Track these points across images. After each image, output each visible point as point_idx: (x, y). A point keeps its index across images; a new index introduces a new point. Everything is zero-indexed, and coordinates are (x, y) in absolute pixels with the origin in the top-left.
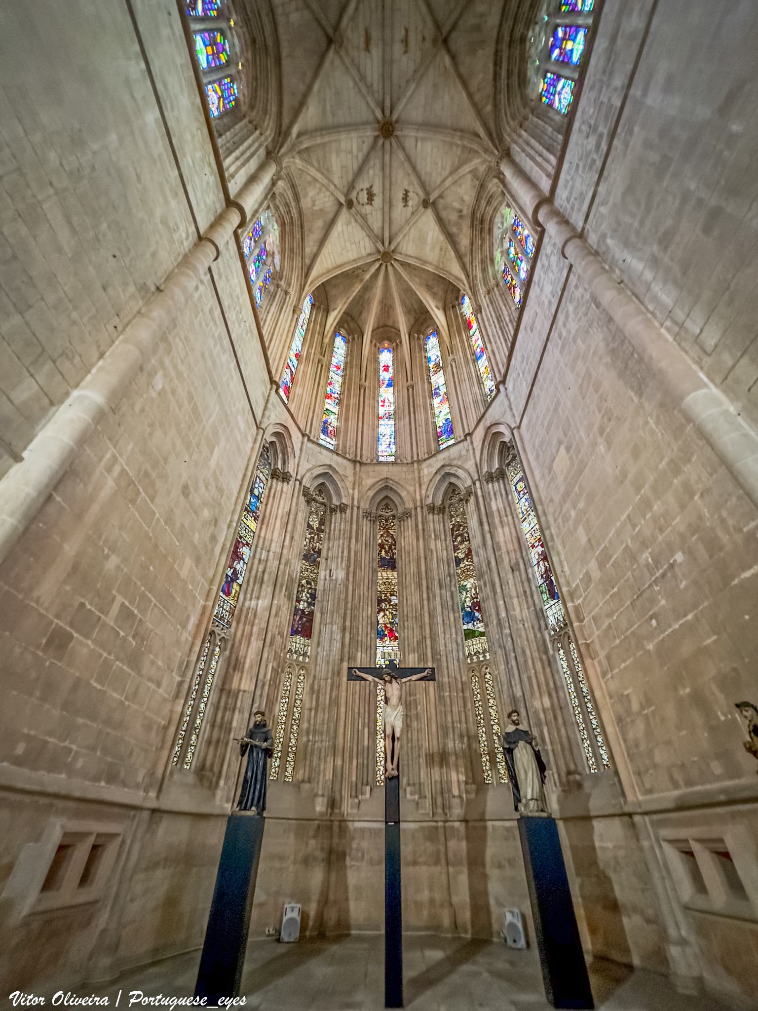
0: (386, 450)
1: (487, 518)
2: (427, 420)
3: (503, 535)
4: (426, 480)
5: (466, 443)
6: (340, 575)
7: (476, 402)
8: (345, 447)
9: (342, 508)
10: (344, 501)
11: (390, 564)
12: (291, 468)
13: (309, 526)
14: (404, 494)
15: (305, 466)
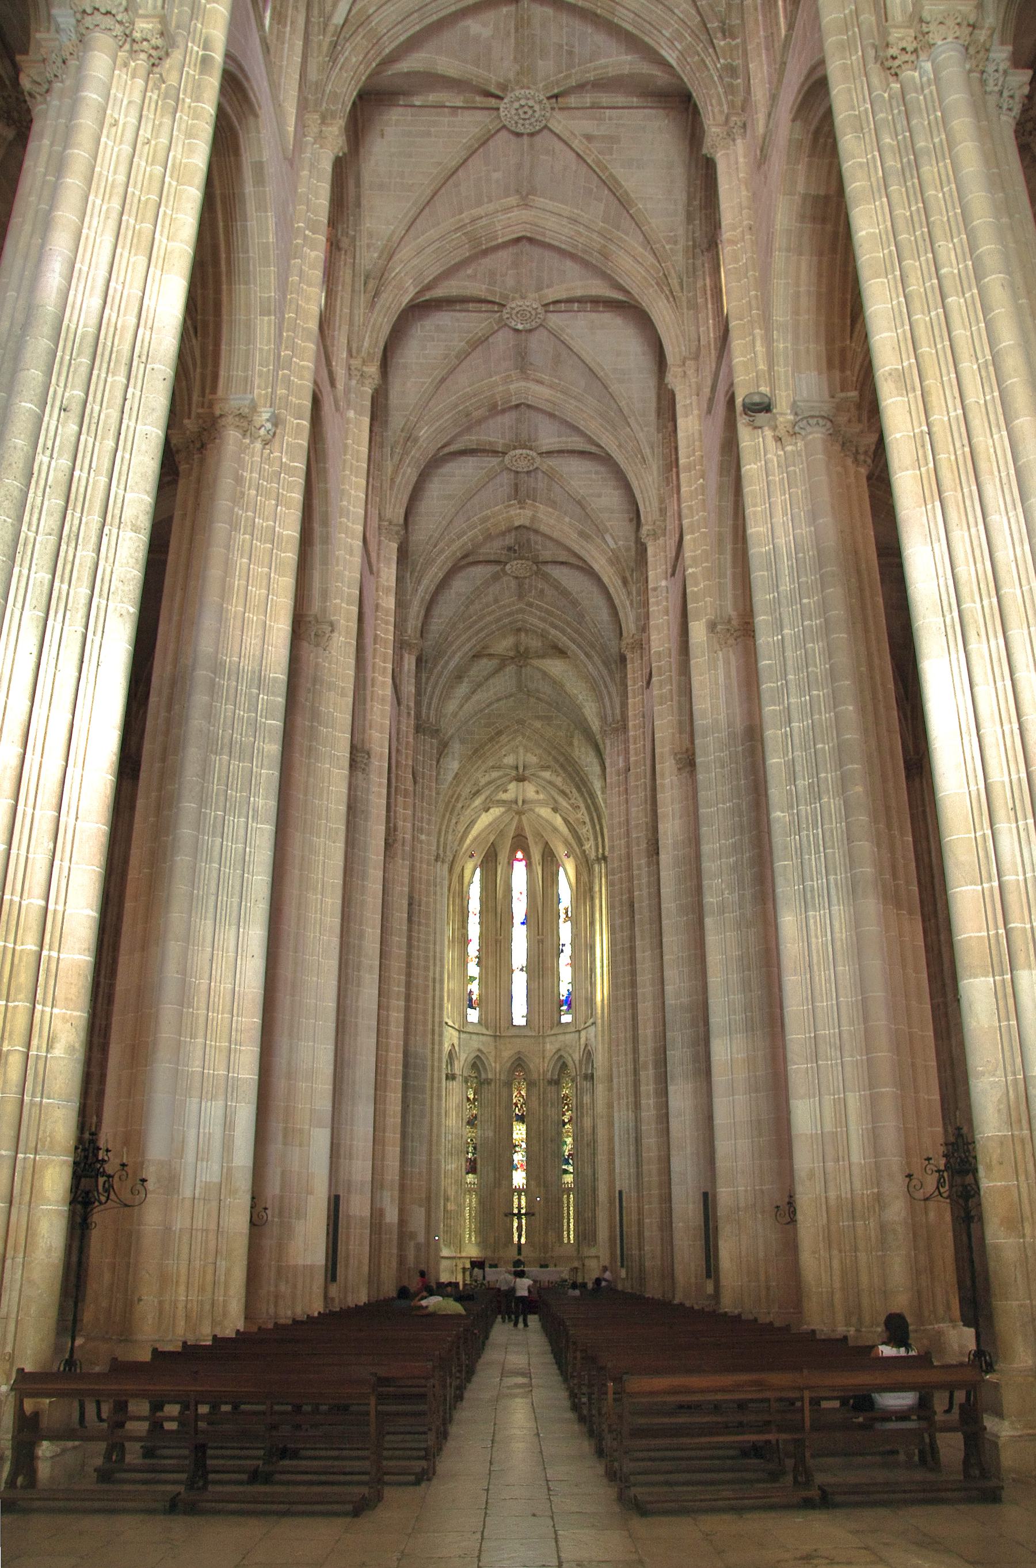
0: (519, 1014)
1: (580, 1107)
2: (553, 987)
3: (587, 1122)
4: (548, 1055)
5: (577, 1034)
6: (491, 1134)
7: (586, 999)
8: (486, 1020)
9: (488, 1082)
10: (490, 1076)
11: (521, 1119)
12: (457, 1071)
13: (468, 1099)
14: (531, 1066)
15: (463, 1057)
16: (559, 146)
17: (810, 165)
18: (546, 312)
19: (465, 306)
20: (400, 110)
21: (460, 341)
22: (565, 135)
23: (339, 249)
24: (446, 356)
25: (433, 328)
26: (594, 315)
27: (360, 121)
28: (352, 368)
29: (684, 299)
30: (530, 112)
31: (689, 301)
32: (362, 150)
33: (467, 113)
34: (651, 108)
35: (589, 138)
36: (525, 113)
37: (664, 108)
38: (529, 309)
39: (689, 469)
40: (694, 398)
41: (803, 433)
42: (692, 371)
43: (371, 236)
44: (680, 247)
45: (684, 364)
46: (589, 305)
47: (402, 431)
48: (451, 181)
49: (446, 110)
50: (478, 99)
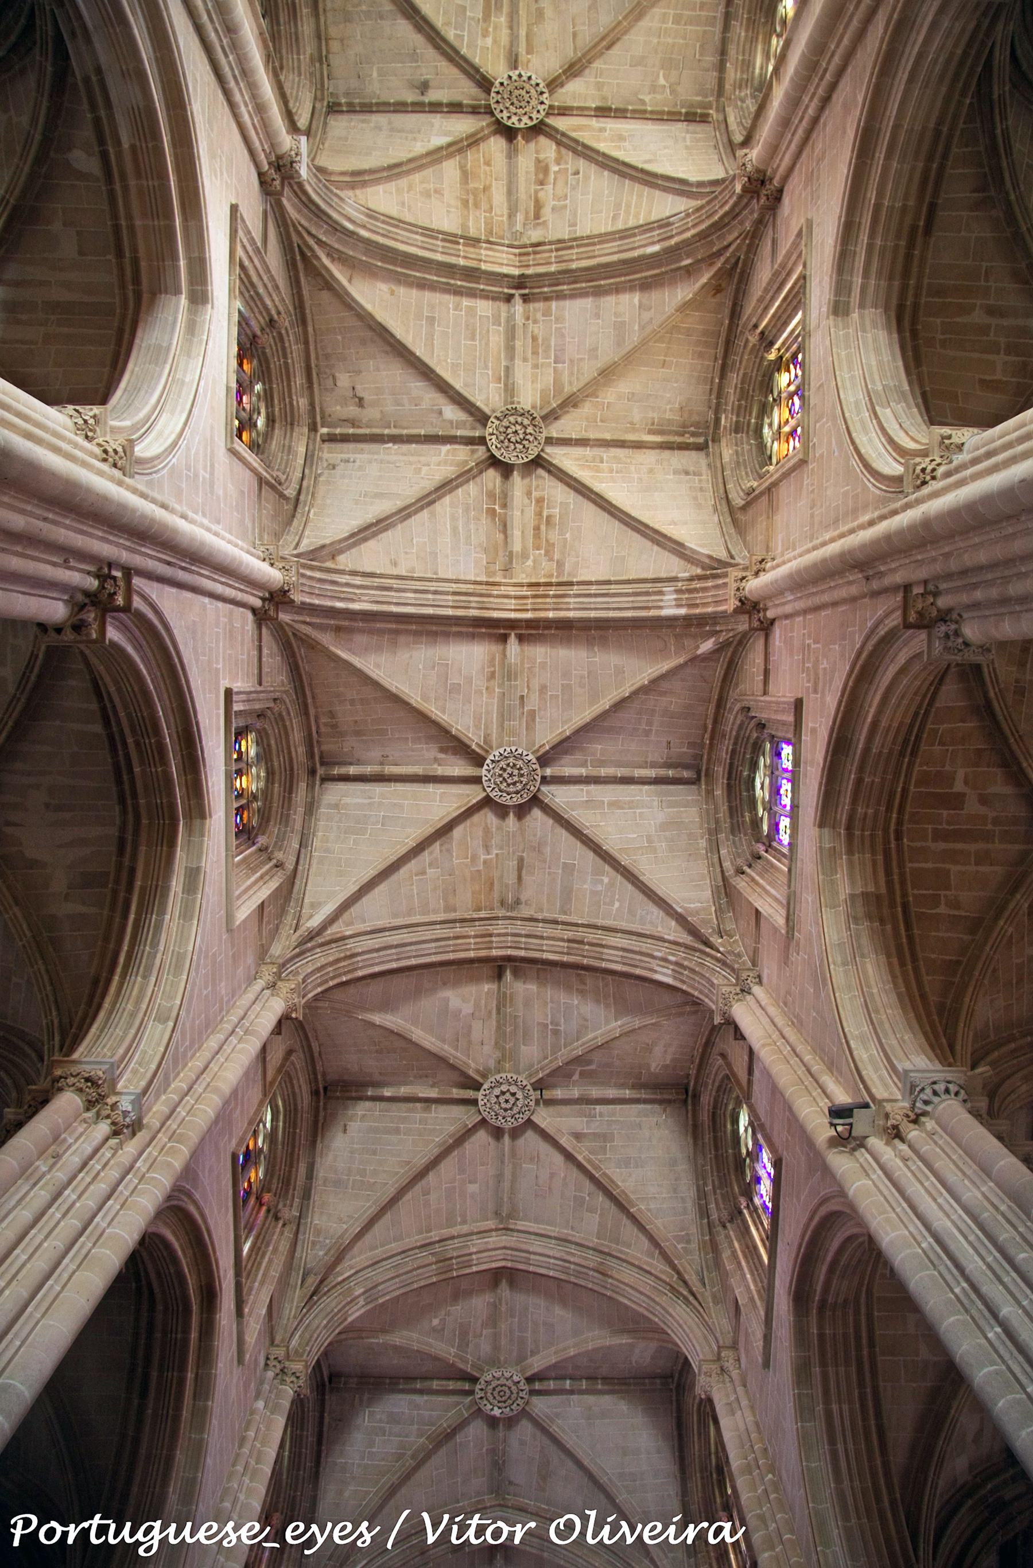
16: (544, 1147)
17: (851, 864)
18: (532, 1392)
19: (427, 1384)
20: (368, 1104)
21: (422, 1436)
22: (551, 1131)
23: (277, 1218)
24: (400, 1457)
25: (384, 1417)
26: (591, 1399)
27: (322, 1114)
28: (272, 1357)
29: (708, 1294)
30: (512, 1100)
31: (714, 1297)
32: (319, 1145)
33: (442, 1108)
34: (645, 1101)
35: (578, 1136)
36: (507, 1101)
37: (660, 1102)
38: (509, 1383)
39: (748, 1470)
40: (740, 1389)
41: (929, 1108)
42: (731, 1361)
43: (318, 1232)
44: (694, 1245)
45: (719, 1358)
46: (584, 1382)
47: (329, 1559)
48: (418, 1188)
49: (418, 1105)
50: (454, 1090)
